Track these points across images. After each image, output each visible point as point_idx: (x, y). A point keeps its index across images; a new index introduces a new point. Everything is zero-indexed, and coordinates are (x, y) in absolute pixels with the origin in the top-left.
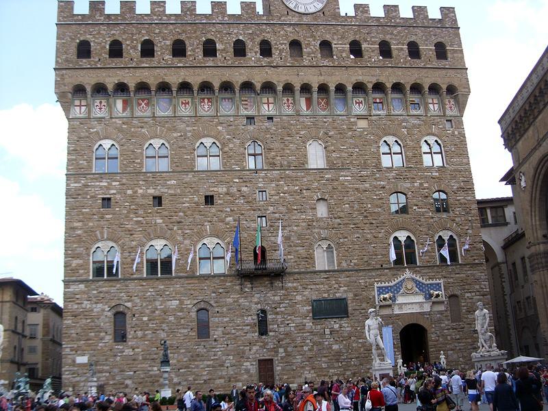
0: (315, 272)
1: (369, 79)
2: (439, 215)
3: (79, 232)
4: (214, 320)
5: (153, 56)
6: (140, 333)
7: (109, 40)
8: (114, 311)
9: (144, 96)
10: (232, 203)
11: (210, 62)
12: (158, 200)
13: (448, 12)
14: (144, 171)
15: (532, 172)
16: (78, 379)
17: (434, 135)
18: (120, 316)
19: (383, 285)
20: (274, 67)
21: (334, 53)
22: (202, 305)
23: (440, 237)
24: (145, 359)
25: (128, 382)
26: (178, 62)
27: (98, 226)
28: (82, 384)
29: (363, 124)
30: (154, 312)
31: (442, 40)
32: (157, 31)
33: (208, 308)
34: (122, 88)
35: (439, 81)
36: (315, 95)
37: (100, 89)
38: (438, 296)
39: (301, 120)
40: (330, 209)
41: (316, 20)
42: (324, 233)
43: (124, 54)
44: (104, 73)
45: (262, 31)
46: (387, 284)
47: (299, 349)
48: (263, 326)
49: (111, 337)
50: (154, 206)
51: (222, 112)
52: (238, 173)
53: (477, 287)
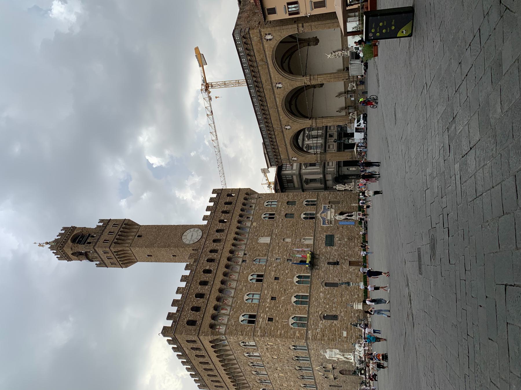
0: (314, 244)
1: (237, 218)
4: (331, 281)
12: (273, 298)
13: (214, 191)
21: (223, 228)
22: (324, 284)
24: (346, 308)
25: (356, 315)
27: (281, 323)
33: (325, 282)
34: (216, 308)
36: (239, 237)
37: (214, 317)
39: (248, 243)
40: (288, 237)
42: (298, 240)
43: (200, 306)
45: (205, 251)
49: (335, 321)
51: (238, 271)
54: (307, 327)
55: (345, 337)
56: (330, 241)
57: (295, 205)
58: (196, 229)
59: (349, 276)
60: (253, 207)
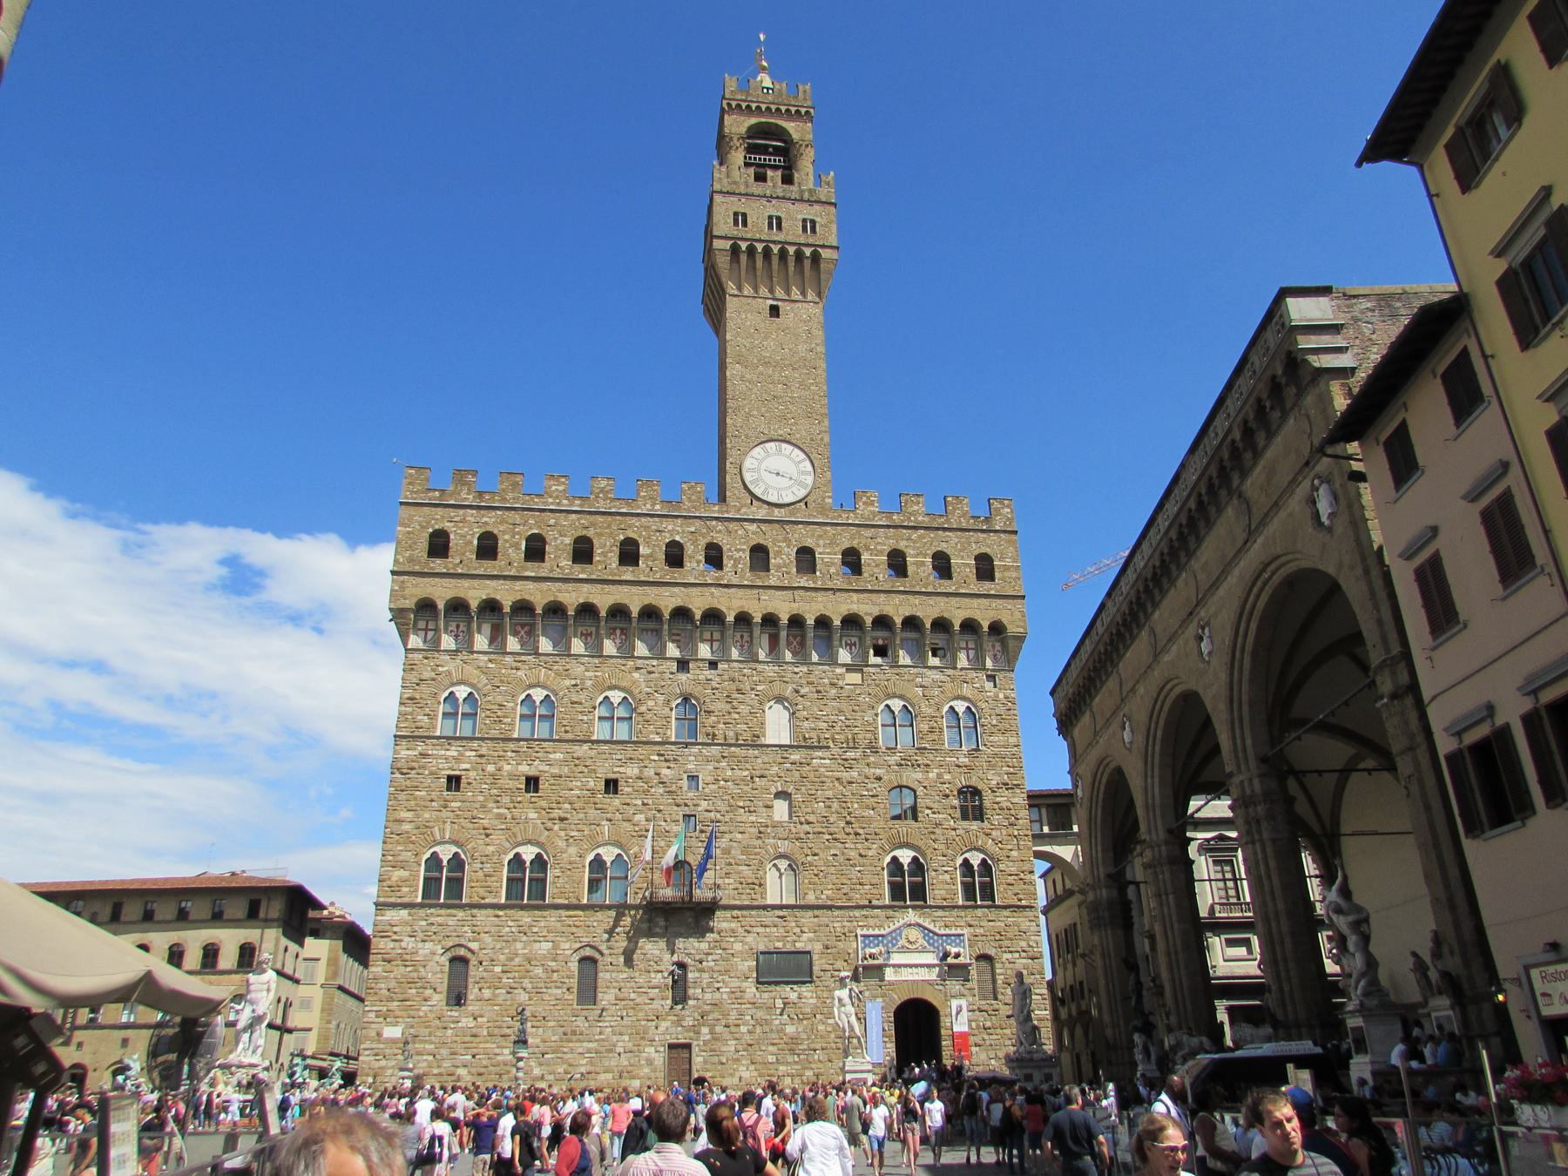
0: (765, 907)
2: (965, 824)
3: (407, 827)
5: (543, 560)
6: (487, 993)
7: (478, 531)
8: (449, 955)
9: (525, 619)
10: (646, 792)
11: (628, 574)
12: (532, 783)
14: (516, 735)
15: (1089, 779)
16: (383, 1063)
17: (964, 698)
18: (459, 963)
19: (871, 932)
20: (726, 586)
22: (588, 952)
23: (966, 861)
25: (462, 1072)
26: (581, 572)
27: (437, 820)
28: (389, 1072)
29: (855, 678)
30: (512, 959)
31: (988, 550)
32: (552, 522)
33: (597, 956)
34: (491, 607)
35: (978, 616)
37: (458, 607)
38: (957, 956)
39: (760, 667)
41: (792, 514)
44: (466, 583)
46: (877, 932)
47: (733, 1029)
48: (679, 989)
49: (443, 996)
50: (527, 791)
52: (657, 748)
53: (1024, 944)
54: (421, 906)
55: (379, 1034)
56: (787, 968)
57: (965, 817)
58: (809, 480)
59: (624, 1042)
60: (934, 661)
